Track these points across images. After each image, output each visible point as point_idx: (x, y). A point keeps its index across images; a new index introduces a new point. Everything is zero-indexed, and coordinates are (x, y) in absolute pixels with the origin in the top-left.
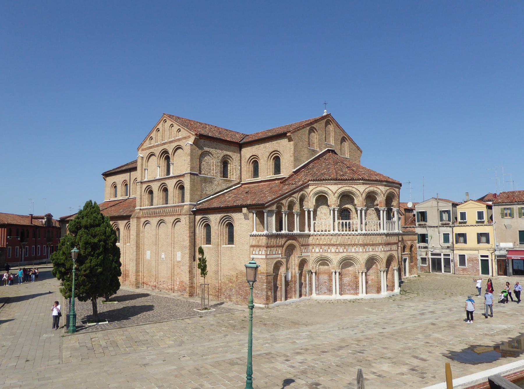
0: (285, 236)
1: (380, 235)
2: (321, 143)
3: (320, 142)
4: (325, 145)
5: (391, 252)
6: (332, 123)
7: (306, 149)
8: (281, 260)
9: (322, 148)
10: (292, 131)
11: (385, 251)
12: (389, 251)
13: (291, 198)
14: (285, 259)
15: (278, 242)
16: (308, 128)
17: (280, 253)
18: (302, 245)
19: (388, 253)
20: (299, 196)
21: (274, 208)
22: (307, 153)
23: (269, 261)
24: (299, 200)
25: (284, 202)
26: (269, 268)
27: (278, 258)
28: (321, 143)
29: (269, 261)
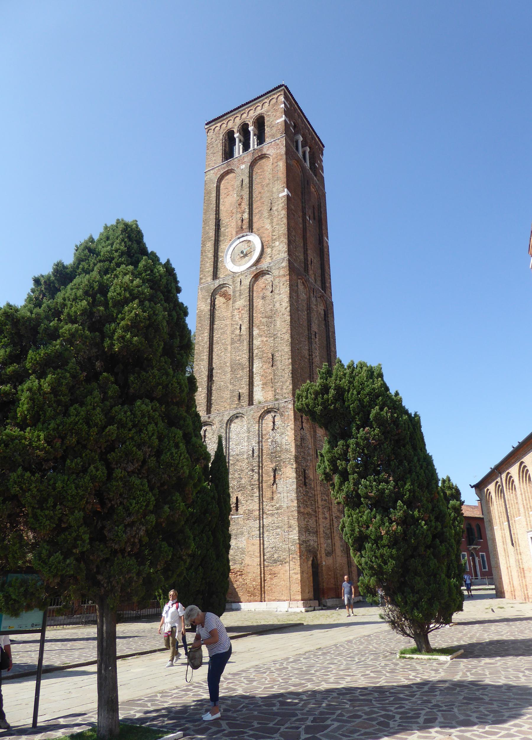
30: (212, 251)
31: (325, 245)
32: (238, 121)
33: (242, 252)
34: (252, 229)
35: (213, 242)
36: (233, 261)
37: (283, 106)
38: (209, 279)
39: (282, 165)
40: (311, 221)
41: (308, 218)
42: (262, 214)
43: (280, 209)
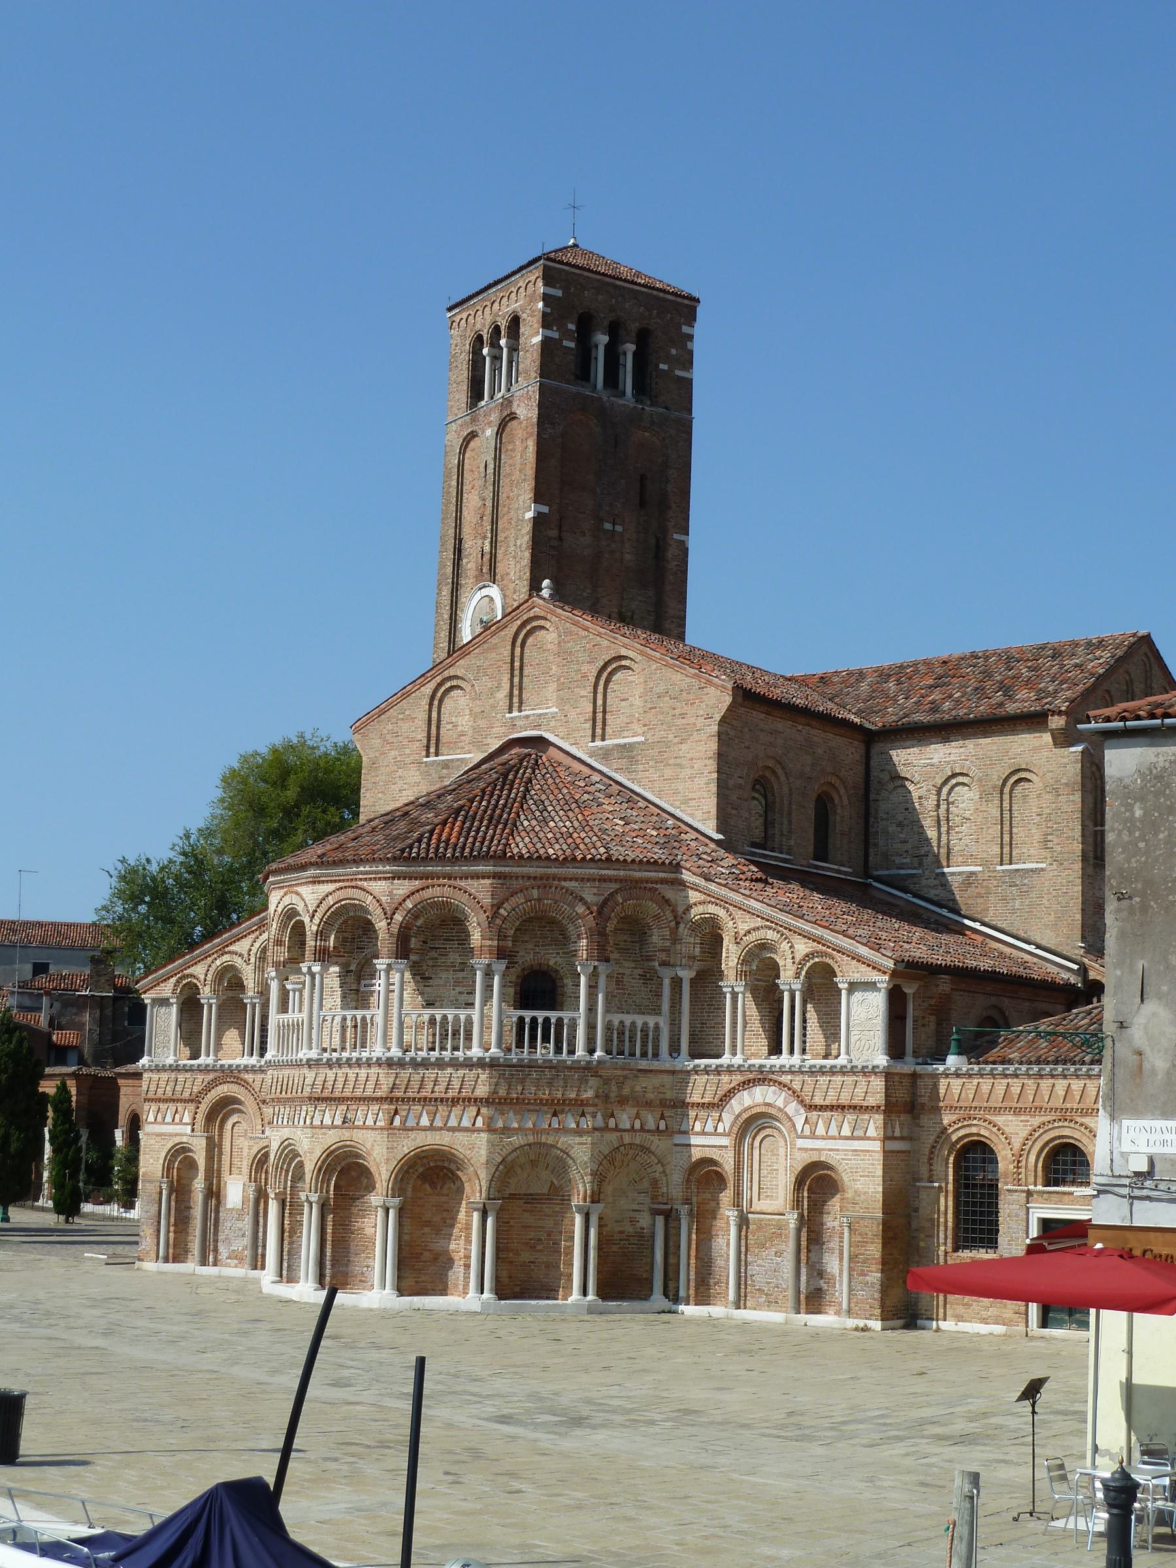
0: (205, 1069)
1: (298, 1065)
2: (482, 723)
4: (504, 725)
5: (346, 1134)
7: (413, 767)
9: (489, 741)
11: (312, 1127)
12: (336, 1127)
13: (226, 958)
17: (187, 1119)
18: (264, 1102)
19: (331, 1138)
21: (167, 989)
22: (417, 778)
23: (153, 1142)
24: (253, 960)
25: (199, 970)
27: (182, 1135)
28: (482, 723)
29: (153, 1142)
32: (489, 319)
35: (450, 586)
37: (541, 305)
39: (531, 445)
40: (619, 528)
41: (608, 526)
42: (508, 547)
43: (524, 546)
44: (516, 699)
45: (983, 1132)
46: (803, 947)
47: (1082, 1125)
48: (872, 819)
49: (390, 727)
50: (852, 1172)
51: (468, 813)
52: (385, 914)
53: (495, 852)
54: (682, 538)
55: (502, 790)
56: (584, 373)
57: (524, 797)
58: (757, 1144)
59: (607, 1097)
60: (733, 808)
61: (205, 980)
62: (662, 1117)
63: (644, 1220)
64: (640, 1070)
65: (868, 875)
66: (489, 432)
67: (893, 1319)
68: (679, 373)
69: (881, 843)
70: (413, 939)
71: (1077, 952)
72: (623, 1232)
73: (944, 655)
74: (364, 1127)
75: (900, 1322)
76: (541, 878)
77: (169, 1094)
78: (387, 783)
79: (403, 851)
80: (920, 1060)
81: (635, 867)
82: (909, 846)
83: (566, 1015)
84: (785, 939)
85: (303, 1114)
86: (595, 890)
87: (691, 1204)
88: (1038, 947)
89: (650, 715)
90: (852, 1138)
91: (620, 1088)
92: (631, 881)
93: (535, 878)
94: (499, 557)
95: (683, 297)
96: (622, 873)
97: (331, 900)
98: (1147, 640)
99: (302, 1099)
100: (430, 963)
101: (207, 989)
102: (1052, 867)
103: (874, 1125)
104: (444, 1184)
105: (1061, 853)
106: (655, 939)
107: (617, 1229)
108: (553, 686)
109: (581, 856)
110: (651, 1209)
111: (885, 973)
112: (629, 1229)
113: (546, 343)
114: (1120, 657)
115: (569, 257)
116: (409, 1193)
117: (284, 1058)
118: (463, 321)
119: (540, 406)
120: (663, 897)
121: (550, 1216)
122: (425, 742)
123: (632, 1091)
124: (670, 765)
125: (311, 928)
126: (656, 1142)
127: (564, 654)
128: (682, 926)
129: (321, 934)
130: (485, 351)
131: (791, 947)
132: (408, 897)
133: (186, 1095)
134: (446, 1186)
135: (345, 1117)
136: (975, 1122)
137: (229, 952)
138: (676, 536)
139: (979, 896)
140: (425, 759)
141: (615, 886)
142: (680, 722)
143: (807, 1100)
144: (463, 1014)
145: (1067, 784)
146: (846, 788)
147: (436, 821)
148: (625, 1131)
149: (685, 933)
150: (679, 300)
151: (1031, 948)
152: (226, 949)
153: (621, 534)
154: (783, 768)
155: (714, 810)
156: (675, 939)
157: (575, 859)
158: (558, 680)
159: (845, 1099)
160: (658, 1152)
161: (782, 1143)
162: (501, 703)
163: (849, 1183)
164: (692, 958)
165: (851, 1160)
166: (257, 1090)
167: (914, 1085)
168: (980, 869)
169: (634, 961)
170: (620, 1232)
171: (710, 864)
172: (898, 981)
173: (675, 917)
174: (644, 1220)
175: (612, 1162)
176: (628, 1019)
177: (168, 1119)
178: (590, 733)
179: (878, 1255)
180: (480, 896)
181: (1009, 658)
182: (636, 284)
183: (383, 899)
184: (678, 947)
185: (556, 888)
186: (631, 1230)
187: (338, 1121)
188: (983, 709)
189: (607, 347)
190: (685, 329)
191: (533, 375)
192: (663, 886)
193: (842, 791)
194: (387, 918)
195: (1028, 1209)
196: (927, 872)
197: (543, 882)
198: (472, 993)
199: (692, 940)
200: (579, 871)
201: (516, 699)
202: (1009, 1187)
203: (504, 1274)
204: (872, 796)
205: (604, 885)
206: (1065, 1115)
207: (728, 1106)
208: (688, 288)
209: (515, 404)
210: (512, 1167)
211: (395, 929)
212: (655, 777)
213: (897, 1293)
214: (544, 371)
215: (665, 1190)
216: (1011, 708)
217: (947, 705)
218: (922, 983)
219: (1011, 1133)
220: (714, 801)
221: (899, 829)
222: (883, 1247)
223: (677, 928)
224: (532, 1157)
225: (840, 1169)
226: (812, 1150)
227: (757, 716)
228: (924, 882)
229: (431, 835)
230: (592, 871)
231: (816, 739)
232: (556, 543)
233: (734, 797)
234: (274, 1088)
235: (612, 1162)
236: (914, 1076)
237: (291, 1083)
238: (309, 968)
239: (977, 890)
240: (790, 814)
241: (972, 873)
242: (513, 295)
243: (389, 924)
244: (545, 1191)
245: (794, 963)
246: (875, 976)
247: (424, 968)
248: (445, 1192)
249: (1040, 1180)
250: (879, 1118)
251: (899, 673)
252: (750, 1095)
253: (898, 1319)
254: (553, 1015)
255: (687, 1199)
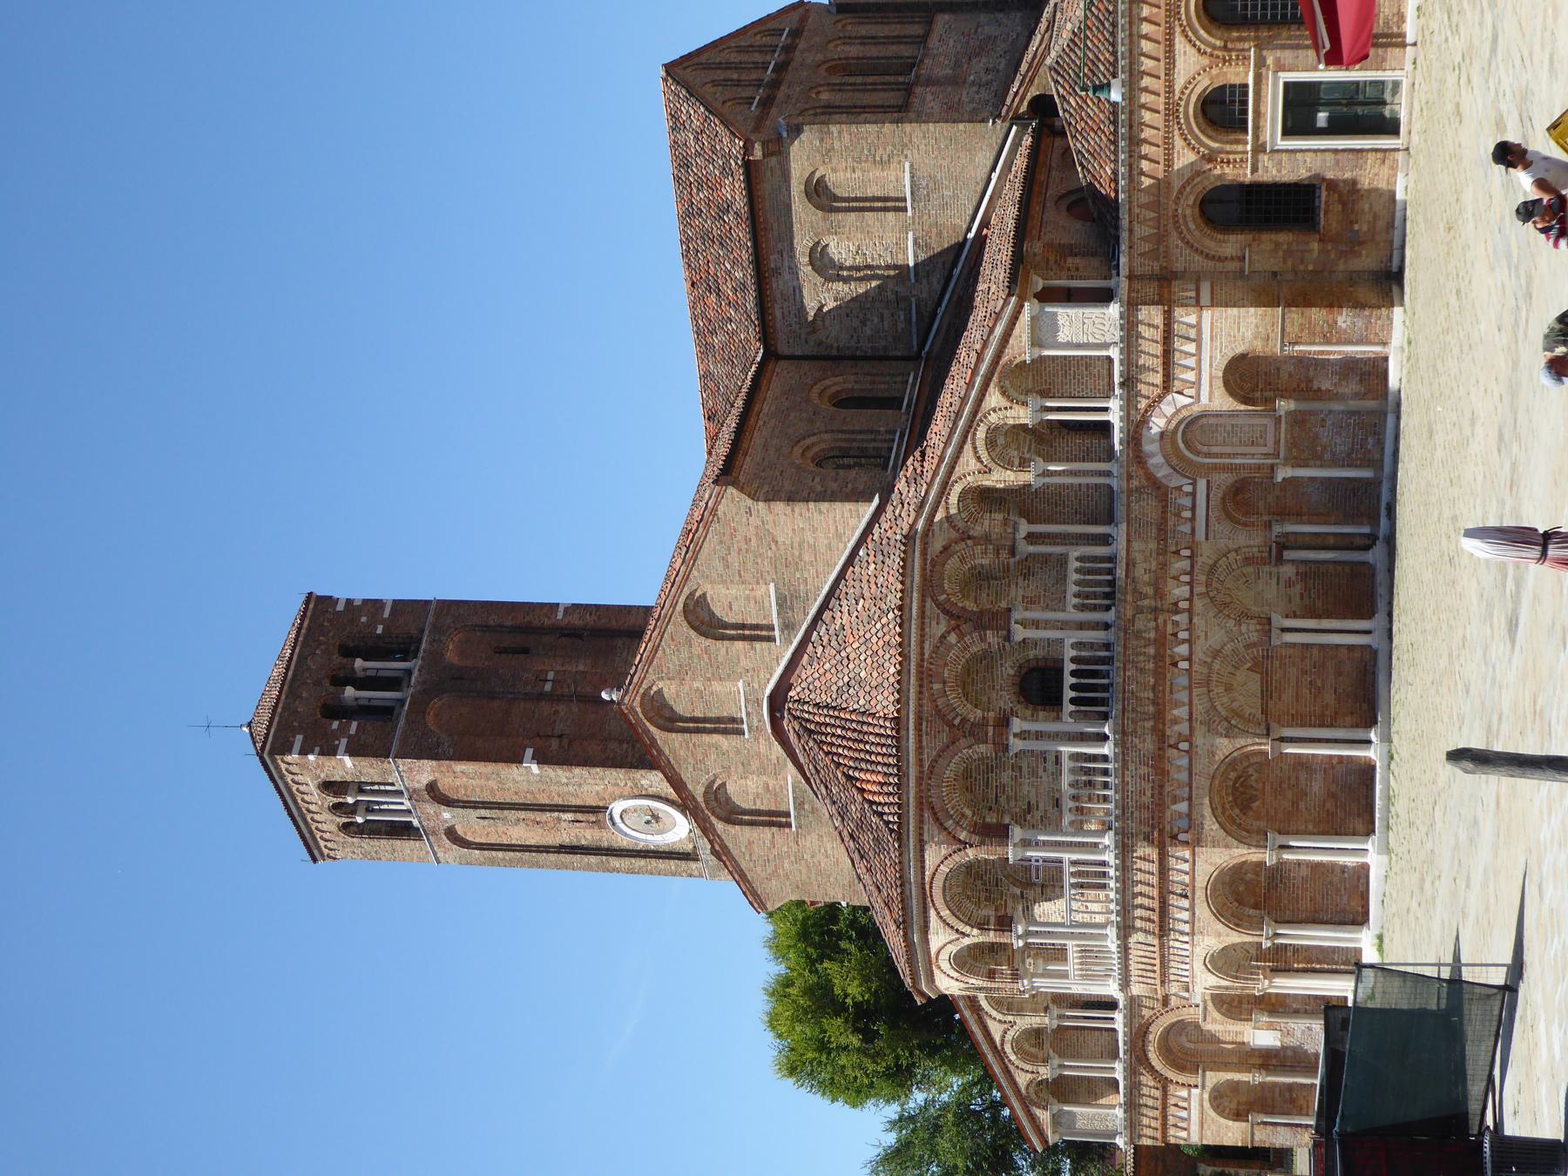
0: (1132, 1072)
1: (1125, 950)
2: (755, 764)
3: (754, 768)
4: (756, 739)
5: (1200, 894)
6: (650, 688)
8: (1208, 1089)
9: (773, 757)
10: (756, 905)
11: (1193, 934)
13: (1008, 1049)
14: (1207, 1073)
15: (1150, 1102)
16: (720, 826)
17: (1184, 1093)
19: (1203, 911)
20: (994, 1013)
24: (1010, 1018)
25: (1022, 1080)
26: (1230, 1134)
27: (1202, 1100)
28: (755, 764)
30: (633, 860)
31: (576, 621)
32: (326, 816)
33: (648, 822)
34: (599, 807)
36: (661, 832)
37: (311, 757)
38: (693, 865)
39: (460, 767)
40: (551, 675)
41: (548, 687)
43: (568, 774)
44: (728, 726)
45: (1191, 202)
46: (994, 399)
47: (1183, 93)
48: (858, 353)
49: (759, 869)
50: (1235, 341)
51: (851, 767)
52: (960, 850)
53: (892, 729)
54: (561, 609)
55: (826, 735)
56: (386, 712)
57: (834, 708)
58: (1205, 449)
59: (1155, 610)
60: (846, 487)
61: (1033, 1072)
62: (1177, 552)
63: (1288, 571)
64: (1127, 576)
65: (918, 357)
66: (447, 814)
67: (1392, 297)
68: (386, 614)
69: (883, 343)
70: (988, 820)
71: (998, 127)
72: (1301, 594)
73: (685, 286)
74: (1192, 873)
75: (1395, 289)
76: (921, 679)
77: (1157, 1113)
78: (819, 873)
79: (892, 831)
80: (1114, 272)
81: (908, 582)
82: (886, 313)
83: (1070, 653)
84: (985, 417)
85: (1177, 944)
86: (934, 623)
87: (1270, 522)
88: (993, 169)
89: (747, 577)
90: (1198, 341)
91: (1146, 597)
92: (924, 585)
93: (921, 686)
94: (579, 802)
95: (306, 609)
96: (915, 595)
97: (945, 913)
98: (672, 69)
99: (1162, 946)
100: (1013, 803)
101: (1042, 1070)
102: (909, 156)
103: (1186, 317)
104: (1252, 787)
105: (894, 146)
106: (985, 562)
107: (1298, 601)
108: (717, 686)
109: (897, 637)
110: (1276, 565)
111: (1022, 306)
112: (1298, 588)
113: (352, 752)
114: (688, 91)
115: (261, 730)
116: (1263, 824)
117: (1115, 956)
118: (329, 845)
119: (419, 758)
120: (941, 552)
121: (1285, 671)
122: (774, 829)
123: (1149, 584)
124: (800, 554)
125: (975, 937)
126: (1204, 559)
127: (681, 674)
128: (971, 533)
129: (982, 926)
130: (360, 820)
131: (994, 411)
132: (941, 824)
133: (1158, 1094)
134: (1254, 785)
135: (1181, 895)
136: (1180, 211)
137: (1002, 1045)
138: (560, 616)
139: (940, 234)
140: (794, 829)
141: (929, 603)
142: (754, 542)
143: (1158, 391)
144: (1067, 764)
145: (822, 140)
146: (825, 379)
147: (859, 798)
148: (1192, 591)
149: (979, 528)
150: (309, 614)
151: (995, 176)
152: (999, 1048)
153: (557, 673)
154: (804, 438)
155: (848, 506)
156: (987, 539)
157: (900, 645)
158: (709, 680)
159: (1158, 349)
160: (1214, 557)
161: (1204, 421)
162: (734, 744)
163: (1247, 345)
164: (1005, 522)
165: (1221, 343)
166: (1151, 1012)
167: (1141, 278)
168: (910, 235)
169: (1009, 586)
170: (1302, 598)
171: (906, 505)
172: (1030, 293)
173: (963, 540)
174: (1288, 571)
175: (1226, 605)
176: (1073, 588)
177: (1184, 1114)
178: (765, 645)
179: (1324, 311)
180: (940, 745)
181: (688, 215)
182: (291, 658)
183: (944, 852)
184: (994, 537)
185: (931, 664)
186: (1298, 587)
187: (1185, 903)
188: (742, 234)
189: (358, 688)
190: (340, 607)
191: (386, 765)
192: (929, 553)
193: (828, 382)
194: (965, 848)
195: (1273, 151)
196: (914, 293)
197: (925, 677)
198: (1043, 756)
199: (986, 523)
200: (913, 639)
201: (728, 726)
202: (1249, 172)
203: (1348, 719)
204: (834, 353)
205: (928, 613)
206: (1171, 112)
207: (1164, 481)
208: (298, 604)
209: (417, 786)
210: (1233, 711)
211: (976, 839)
212: (812, 571)
213: (1363, 292)
214: (382, 752)
215: (1255, 550)
216: (740, 203)
217: (740, 275)
218: (1032, 272)
219: (1192, 170)
220: (838, 505)
221: (869, 323)
222: (1314, 306)
223: (974, 538)
224: (1221, 690)
225: (1231, 355)
226: (1211, 386)
227: (747, 464)
228: (924, 295)
229: (875, 803)
230: (913, 626)
231: (773, 408)
232: (565, 742)
233: (834, 486)
234: (1149, 981)
235: (1226, 605)
236: (1130, 277)
237: (1144, 960)
238: (1019, 937)
239: (933, 238)
240: (853, 432)
241: (915, 242)
242: (302, 788)
243: (971, 846)
244: (1258, 677)
245: (1011, 408)
246: (1025, 317)
247: (1018, 810)
248: (1260, 786)
249: (1241, 137)
250: (1179, 312)
251: (704, 333)
252: (1152, 455)
253: (1391, 290)
254: (1069, 667)
255: (1265, 527)
